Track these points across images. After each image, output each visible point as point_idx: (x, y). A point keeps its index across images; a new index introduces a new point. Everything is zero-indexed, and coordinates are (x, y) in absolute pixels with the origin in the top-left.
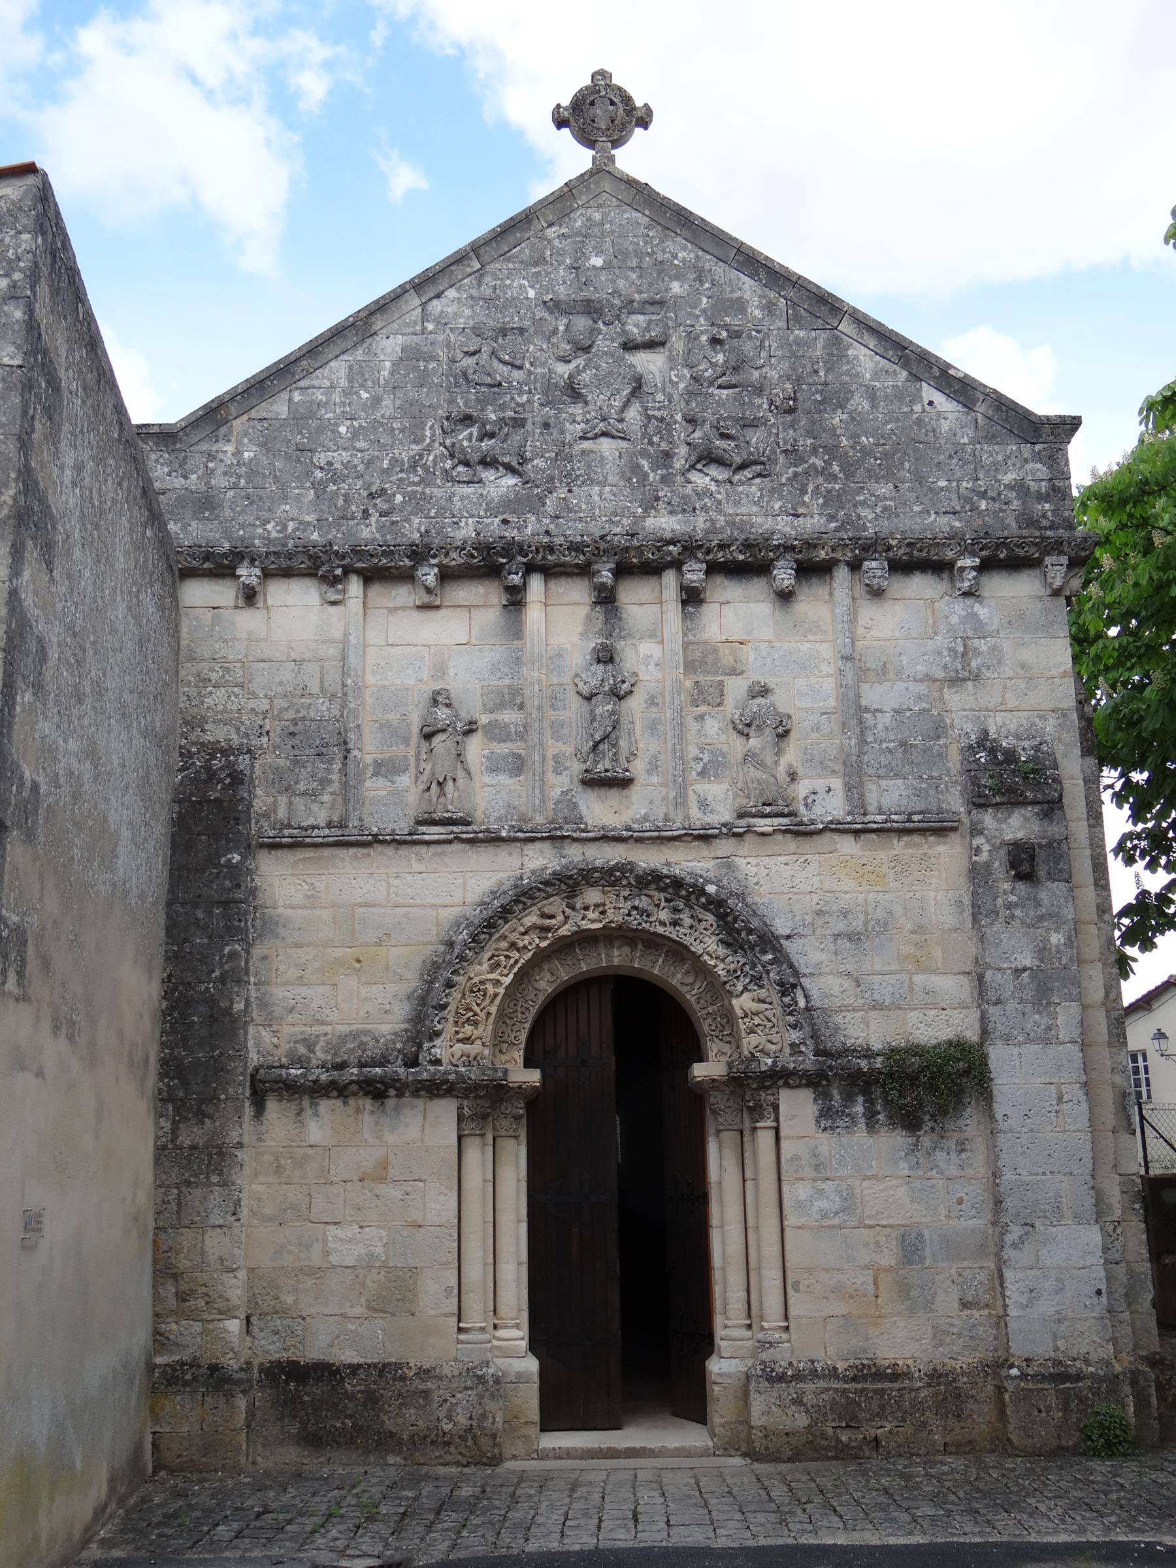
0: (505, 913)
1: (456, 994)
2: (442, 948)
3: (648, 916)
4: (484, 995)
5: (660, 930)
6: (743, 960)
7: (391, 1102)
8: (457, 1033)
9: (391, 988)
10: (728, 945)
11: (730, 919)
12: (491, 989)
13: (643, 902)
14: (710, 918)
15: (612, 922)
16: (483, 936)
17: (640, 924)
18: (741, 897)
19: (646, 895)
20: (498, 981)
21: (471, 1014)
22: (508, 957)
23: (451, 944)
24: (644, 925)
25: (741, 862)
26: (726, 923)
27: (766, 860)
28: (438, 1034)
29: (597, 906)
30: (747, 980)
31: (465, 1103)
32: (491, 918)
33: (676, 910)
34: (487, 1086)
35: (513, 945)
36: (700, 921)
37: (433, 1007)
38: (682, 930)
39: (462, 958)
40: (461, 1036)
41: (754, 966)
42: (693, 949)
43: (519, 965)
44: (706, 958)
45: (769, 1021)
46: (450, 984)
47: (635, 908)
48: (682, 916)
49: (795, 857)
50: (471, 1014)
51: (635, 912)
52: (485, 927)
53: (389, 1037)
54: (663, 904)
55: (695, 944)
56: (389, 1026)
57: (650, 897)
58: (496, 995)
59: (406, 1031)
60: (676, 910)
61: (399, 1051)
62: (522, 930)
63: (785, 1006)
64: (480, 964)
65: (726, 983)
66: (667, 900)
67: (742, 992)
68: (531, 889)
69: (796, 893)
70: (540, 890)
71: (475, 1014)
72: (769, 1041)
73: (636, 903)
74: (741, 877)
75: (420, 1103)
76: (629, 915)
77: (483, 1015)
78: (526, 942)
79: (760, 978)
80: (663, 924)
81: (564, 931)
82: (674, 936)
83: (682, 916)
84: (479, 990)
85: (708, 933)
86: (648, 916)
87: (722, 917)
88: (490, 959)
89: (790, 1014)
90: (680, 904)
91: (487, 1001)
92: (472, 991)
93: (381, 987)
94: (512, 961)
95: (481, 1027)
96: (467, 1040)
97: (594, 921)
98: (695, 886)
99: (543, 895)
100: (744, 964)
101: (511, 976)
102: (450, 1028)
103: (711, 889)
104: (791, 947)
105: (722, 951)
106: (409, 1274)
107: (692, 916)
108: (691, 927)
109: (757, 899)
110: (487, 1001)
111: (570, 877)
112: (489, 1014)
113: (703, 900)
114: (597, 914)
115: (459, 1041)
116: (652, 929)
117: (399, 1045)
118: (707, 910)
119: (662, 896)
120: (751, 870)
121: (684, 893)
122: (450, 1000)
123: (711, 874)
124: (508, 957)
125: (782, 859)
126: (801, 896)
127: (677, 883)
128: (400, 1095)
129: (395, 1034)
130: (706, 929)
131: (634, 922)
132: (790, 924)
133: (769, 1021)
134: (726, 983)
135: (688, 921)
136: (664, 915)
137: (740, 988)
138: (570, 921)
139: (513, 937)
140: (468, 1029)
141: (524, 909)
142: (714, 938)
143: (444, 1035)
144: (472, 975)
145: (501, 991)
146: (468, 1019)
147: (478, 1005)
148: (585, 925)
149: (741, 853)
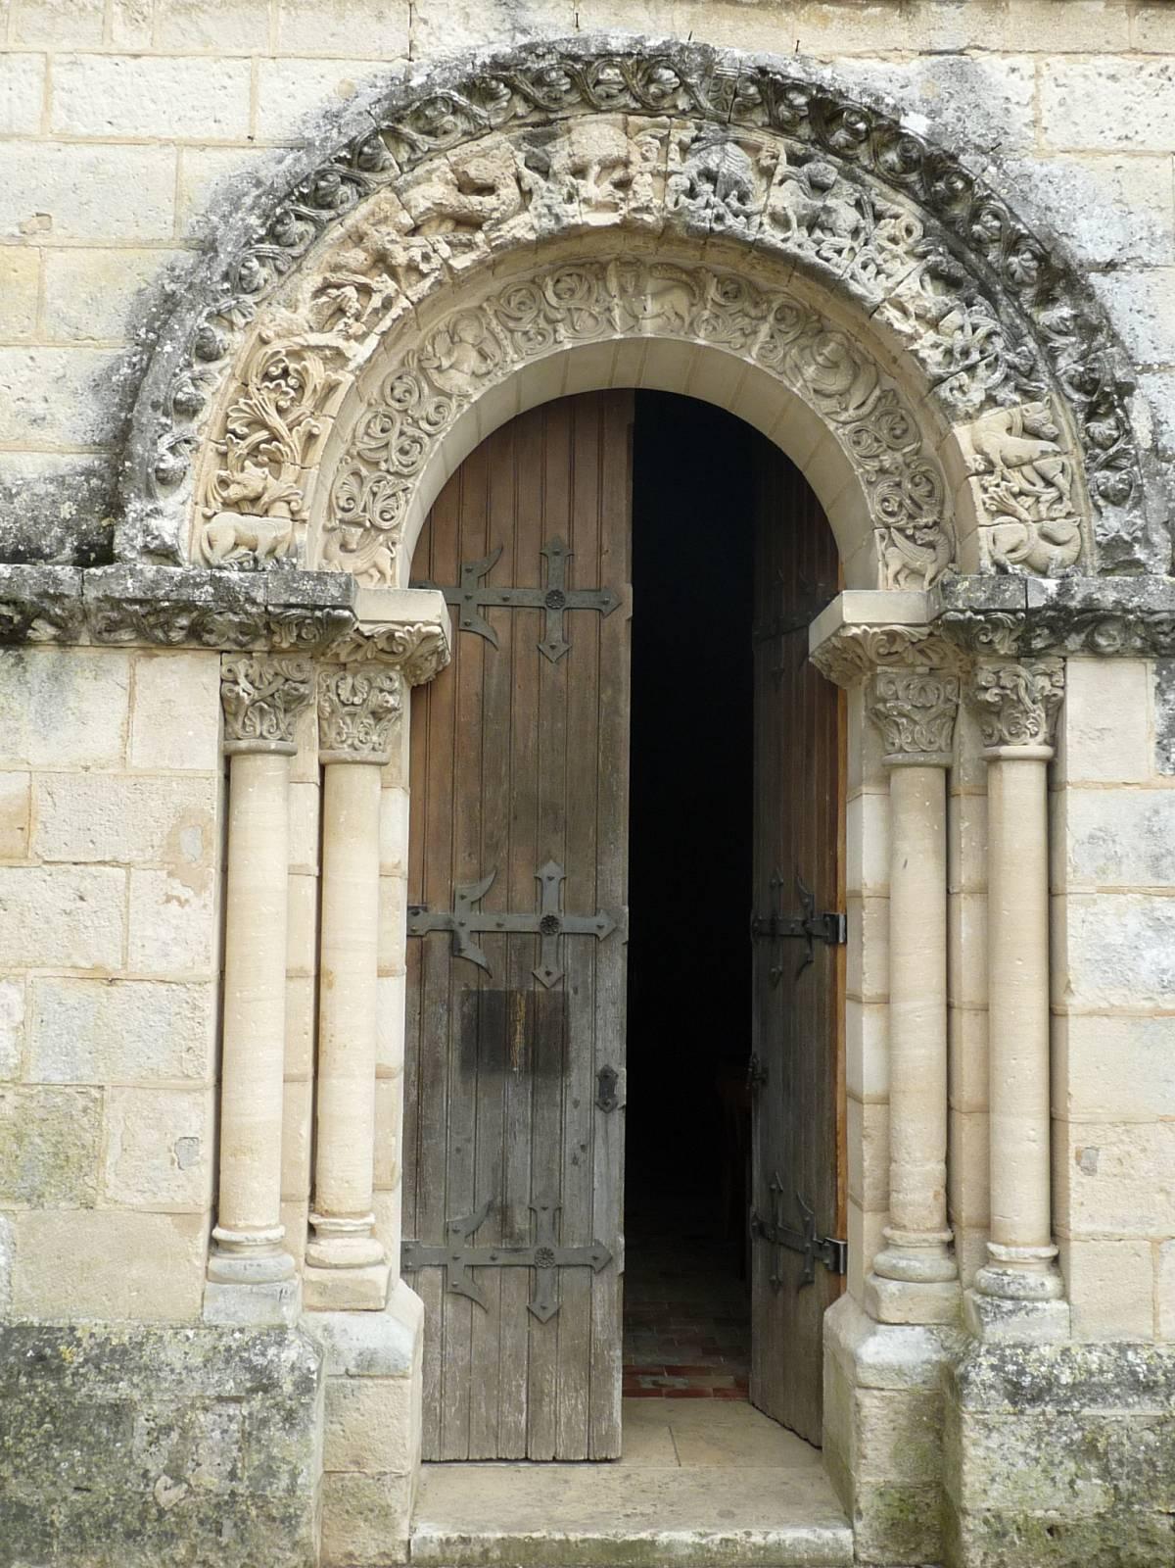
0: (359, 162)
1: (220, 378)
2: (187, 259)
3: (743, 198)
4: (301, 388)
5: (773, 236)
6: (988, 324)
7: (42, 659)
8: (224, 483)
9: (54, 359)
10: (950, 283)
11: (959, 210)
12: (317, 372)
13: (732, 161)
14: (908, 211)
15: (647, 209)
16: (299, 227)
17: (719, 218)
18: (994, 152)
19: (737, 142)
20: (339, 353)
21: (264, 434)
22: (365, 290)
23: (208, 248)
24: (730, 220)
25: (992, 66)
26: (949, 224)
27: (1059, 63)
28: (167, 480)
29: (609, 165)
30: (998, 376)
31: (241, 667)
32: (322, 175)
33: (819, 188)
34: (300, 623)
35: (381, 261)
36: (878, 217)
37: (155, 406)
38: (830, 240)
39: (240, 282)
40: (234, 492)
41: (1015, 341)
42: (856, 288)
43: (395, 312)
44: (891, 314)
45: (1049, 483)
46: (206, 353)
47: (709, 176)
48: (831, 202)
49: (1136, 61)
50: (264, 434)
51: (708, 187)
52: (303, 198)
53: (41, 489)
54: (783, 168)
55: (863, 275)
56: (40, 459)
57: (753, 149)
58: (331, 388)
59: (89, 473)
60: (819, 188)
61: (68, 526)
62: (406, 220)
63: (1092, 443)
64: (292, 305)
65: (940, 380)
66: (795, 160)
67: (981, 409)
68: (432, 102)
69: (1132, 154)
70: (456, 110)
71: (275, 437)
72: (1047, 537)
73: (712, 166)
74: (992, 105)
75: (119, 665)
76: (692, 193)
77: (295, 439)
78: (416, 253)
79: (1030, 373)
80: (781, 221)
81: (522, 227)
82: (809, 254)
83: (831, 202)
84: (285, 373)
85: (900, 249)
86: (743, 198)
87: (935, 206)
88: (321, 291)
89: (1109, 465)
90: (827, 169)
91: (308, 403)
92: (267, 377)
93: (22, 354)
94: (376, 301)
95: (289, 473)
96: (249, 504)
97: (600, 206)
98: (872, 114)
99: (462, 124)
100: (989, 336)
101: (373, 341)
102: (202, 469)
103: (915, 125)
104: (1115, 294)
105: (932, 298)
106: (81, 1102)
107: (858, 205)
108: (855, 232)
109: (1031, 164)
110: (308, 403)
111: (539, 80)
112: (311, 437)
113: (892, 157)
114: (607, 186)
115: (227, 505)
116: (752, 234)
117: (67, 510)
118: (898, 185)
119: (781, 145)
120: (1019, 88)
121: (841, 136)
122: (206, 393)
123: (914, 93)
124: (365, 290)
125: (1100, 61)
126: (1147, 163)
127: (826, 109)
128: (64, 640)
129: (60, 481)
130: (894, 240)
131: (703, 212)
132: (1116, 234)
133: (1049, 483)
134: (940, 380)
135: (847, 217)
136: (787, 197)
137: (977, 396)
138: (536, 202)
139: (382, 236)
140: (254, 477)
141: (413, 163)
142: (912, 264)
143: (188, 485)
144: (268, 333)
145: (346, 378)
146: (255, 451)
147: (280, 411)
148: (577, 215)
149: (994, 41)
